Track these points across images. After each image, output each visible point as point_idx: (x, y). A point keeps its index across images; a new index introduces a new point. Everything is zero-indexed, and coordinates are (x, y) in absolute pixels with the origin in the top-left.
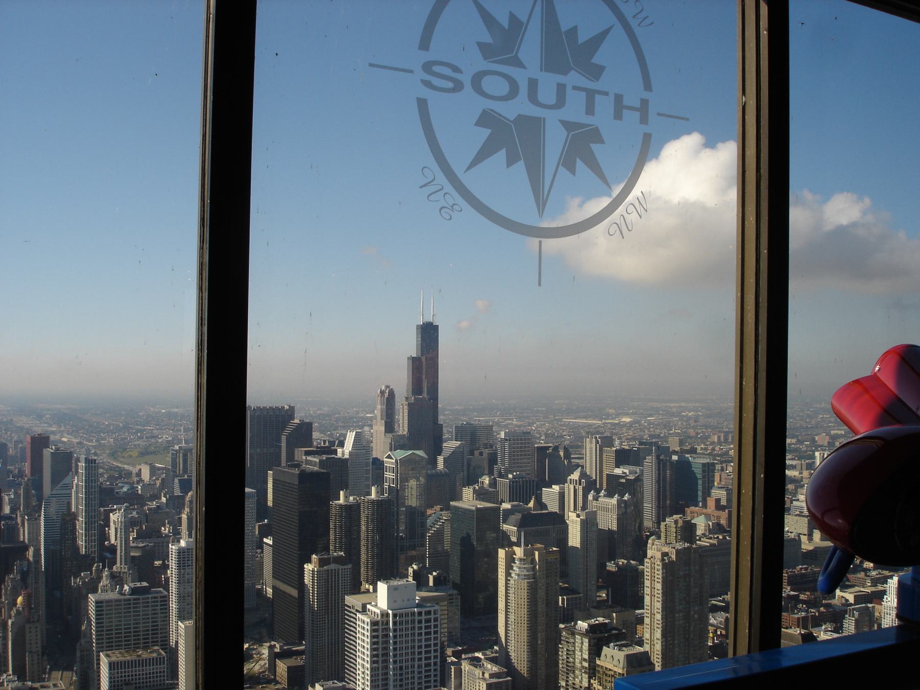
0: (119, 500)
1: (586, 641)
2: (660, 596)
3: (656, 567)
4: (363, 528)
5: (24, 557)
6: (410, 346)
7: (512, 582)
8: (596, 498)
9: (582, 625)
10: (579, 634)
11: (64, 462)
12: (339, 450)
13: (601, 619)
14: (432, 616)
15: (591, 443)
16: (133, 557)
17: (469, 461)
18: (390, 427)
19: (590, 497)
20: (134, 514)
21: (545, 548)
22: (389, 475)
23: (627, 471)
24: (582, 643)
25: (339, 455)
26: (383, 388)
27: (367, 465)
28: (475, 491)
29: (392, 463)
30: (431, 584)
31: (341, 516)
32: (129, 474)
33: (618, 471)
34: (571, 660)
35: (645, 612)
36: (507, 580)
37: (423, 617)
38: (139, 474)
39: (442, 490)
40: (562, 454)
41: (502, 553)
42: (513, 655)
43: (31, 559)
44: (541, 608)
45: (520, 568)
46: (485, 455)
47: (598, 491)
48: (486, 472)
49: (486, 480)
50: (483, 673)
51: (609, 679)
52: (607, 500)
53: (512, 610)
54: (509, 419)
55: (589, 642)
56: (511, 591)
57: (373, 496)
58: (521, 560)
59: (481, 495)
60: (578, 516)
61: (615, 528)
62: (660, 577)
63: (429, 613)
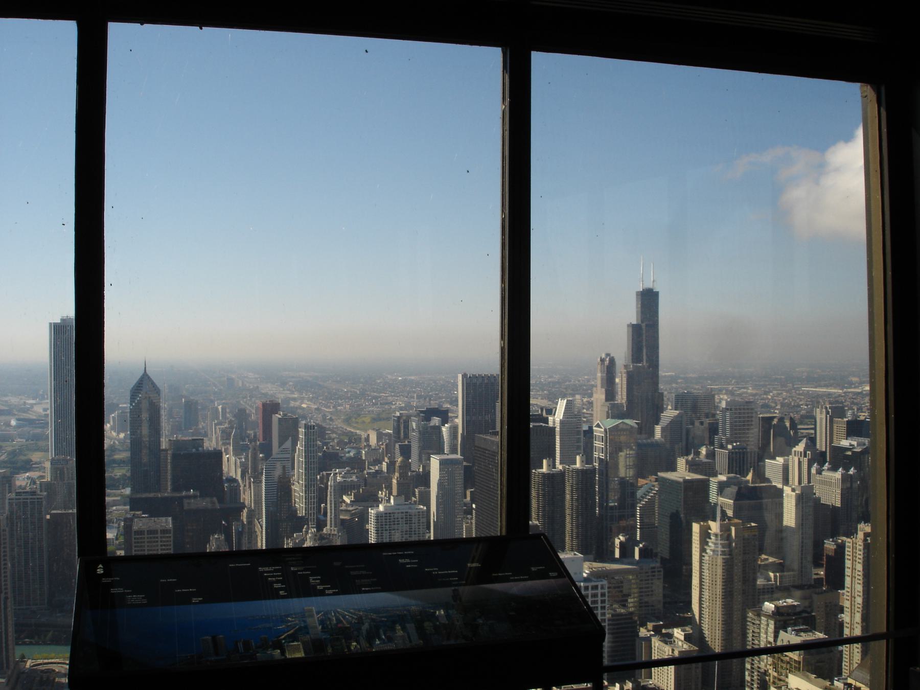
0: (341, 465)
1: (772, 623)
2: (861, 578)
3: (858, 547)
4: (568, 497)
5: (238, 517)
6: (630, 314)
7: (706, 558)
8: (819, 472)
9: (769, 606)
10: (765, 616)
11: (290, 427)
12: (551, 418)
13: (790, 601)
14: (599, 591)
15: (821, 413)
16: (343, 520)
17: (688, 431)
18: (610, 395)
19: (813, 471)
20: (354, 478)
21: (743, 524)
22: (598, 444)
23: (855, 443)
24: (768, 625)
25: (551, 424)
26: (603, 356)
27: (578, 433)
28: (687, 462)
29: (601, 432)
30: (637, 557)
31: (544, 485)
32: (358, 439)
33: (845, 443)
34: (756, 642)
35: (845, 594)
36: (701, 556)
37: (590, 592)
38: (367, 439)
39: (653, 459)
40: (788, 424)
41: (696, 527)
42: (706, 632)
43: (245, 520)
44: (738, 585)
45: (715, 544)
46: (706, 425)
47: (822, 464)
48: (707, 442)
49: (703, 451)
50: (673, 650)
51: (784, 666)
52: (831, 474)
53: (706, 587)
54: (744, 388)
55: (775, 624)
56: (706, 566)
57: (578, 465)
58: (716, 535)
59: (693, 466)
60: (793, 490)
61: (838, 504)
62: (861, 557)
63: (596, 587)
